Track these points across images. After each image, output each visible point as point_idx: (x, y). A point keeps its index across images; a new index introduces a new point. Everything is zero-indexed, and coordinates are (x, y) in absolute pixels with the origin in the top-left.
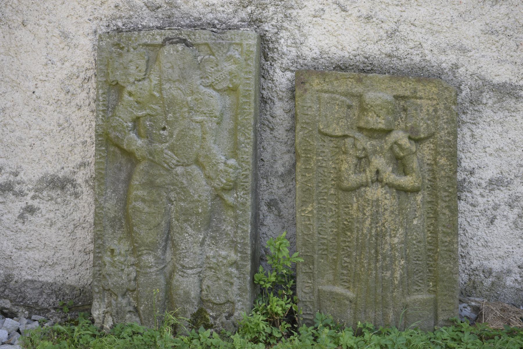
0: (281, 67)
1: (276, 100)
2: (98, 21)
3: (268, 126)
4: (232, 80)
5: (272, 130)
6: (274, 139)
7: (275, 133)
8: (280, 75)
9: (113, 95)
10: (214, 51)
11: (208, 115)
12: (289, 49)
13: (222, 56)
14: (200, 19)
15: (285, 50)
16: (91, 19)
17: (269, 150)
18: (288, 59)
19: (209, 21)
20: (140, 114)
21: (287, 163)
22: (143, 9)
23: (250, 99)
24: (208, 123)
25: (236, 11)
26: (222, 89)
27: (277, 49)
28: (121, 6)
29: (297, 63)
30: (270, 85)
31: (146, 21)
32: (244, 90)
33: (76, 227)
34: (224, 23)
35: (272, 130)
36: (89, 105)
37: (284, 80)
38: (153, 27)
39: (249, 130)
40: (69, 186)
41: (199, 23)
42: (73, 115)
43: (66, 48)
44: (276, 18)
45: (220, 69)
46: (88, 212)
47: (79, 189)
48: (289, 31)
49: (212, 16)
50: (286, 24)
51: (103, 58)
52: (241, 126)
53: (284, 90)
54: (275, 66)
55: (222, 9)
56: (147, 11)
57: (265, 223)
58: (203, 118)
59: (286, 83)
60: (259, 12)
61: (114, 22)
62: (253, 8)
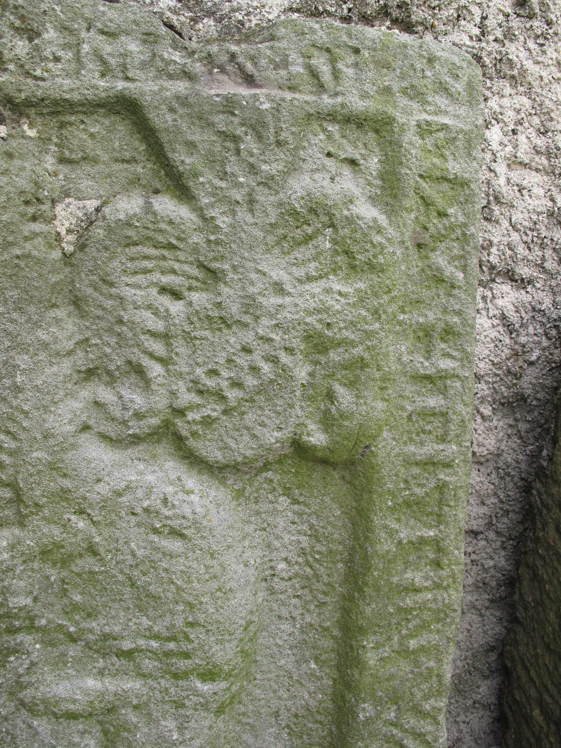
4: (330, 396)
11: (148, 664)
12: (516, 175)
13: (251, 202)
23: (440, 519)
24: (150, 719)
26: (248, 462)
29: (542, 246)
32: (408, 462)
34: (210, 14)
45: (234, 309)
48: (528, 94)
50: (523, 54)
52: (377, 702)
59: (493, 334)
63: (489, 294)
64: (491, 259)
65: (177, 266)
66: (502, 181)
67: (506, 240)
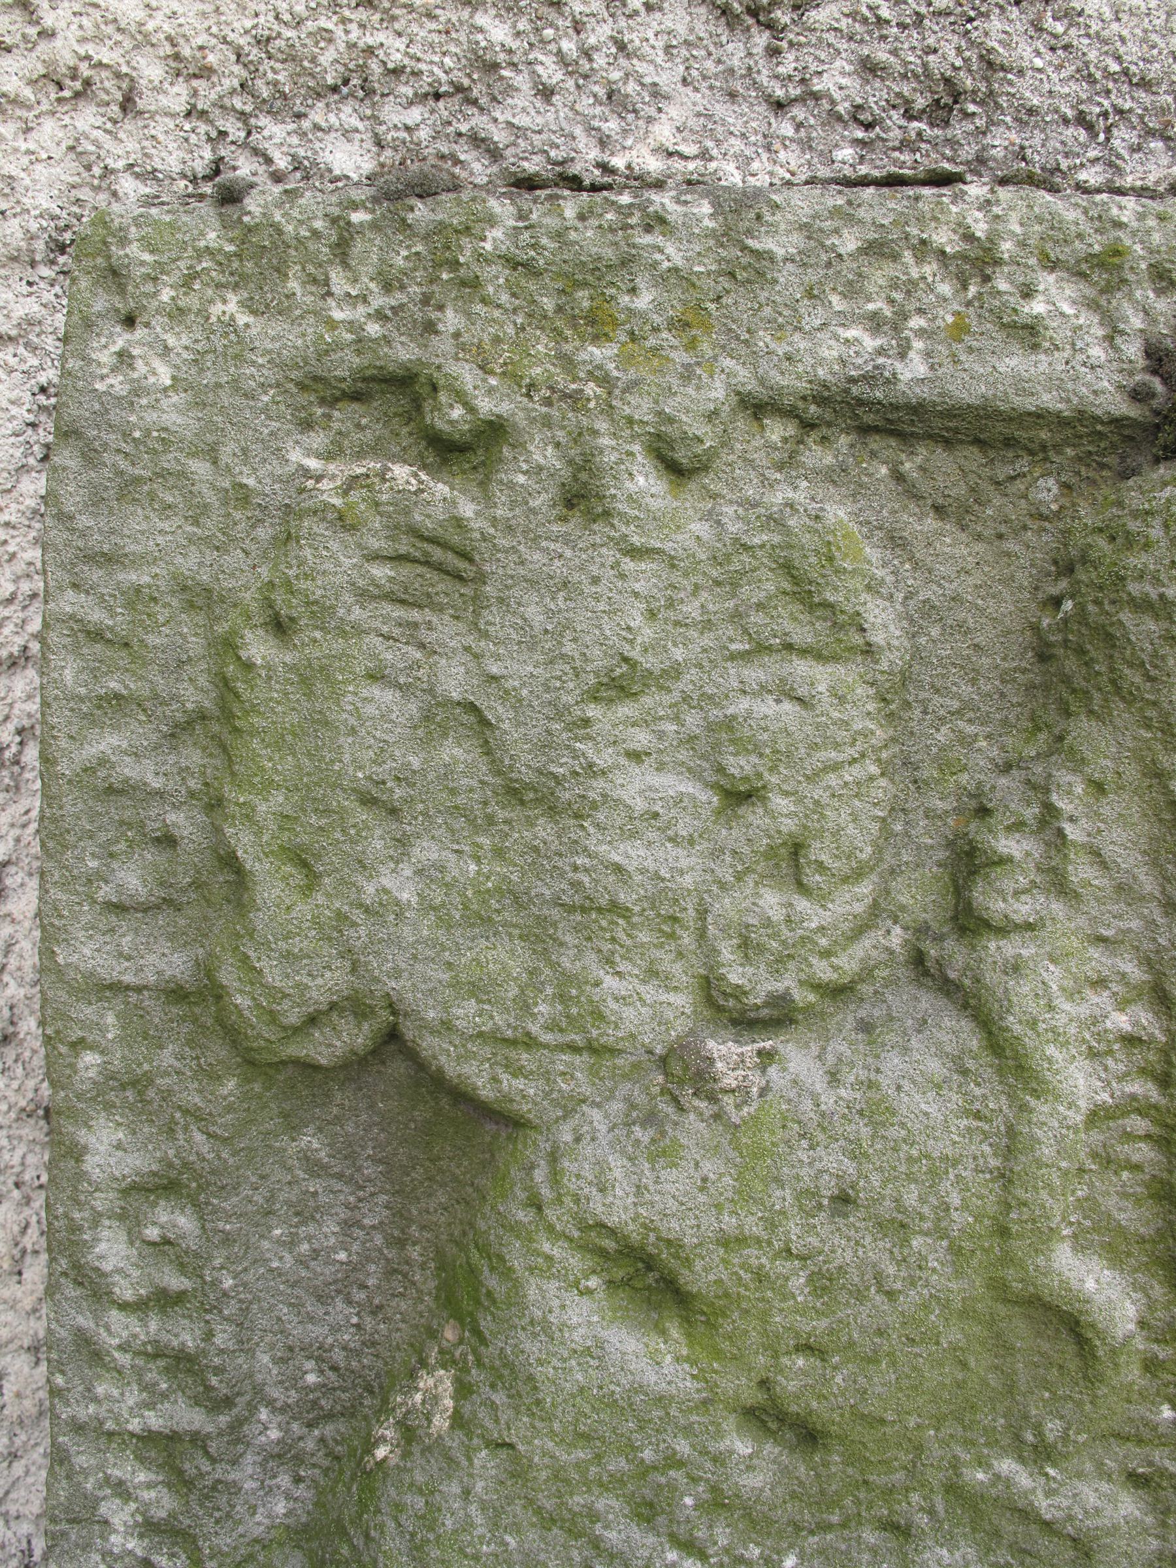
2: (87, 118)
9: (305, 1212)
31: (663, 132)
51: (136, 597)
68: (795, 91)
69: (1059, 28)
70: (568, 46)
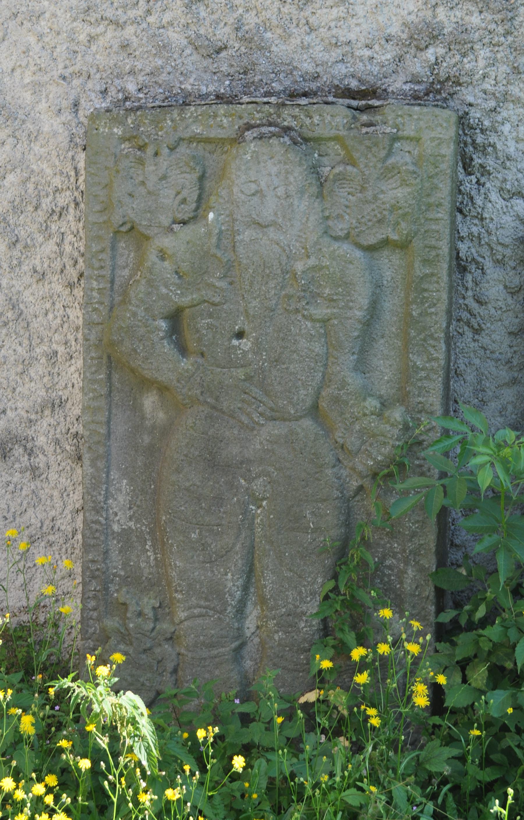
0: (501, 189)
1: (488, 264)
3: (468, 324)
5: (477, 331)
6: (482, 352)
7: (485, 340)
8: (498, 206)
10: (356, 155)
14: (316, 77)
15: (512, 150)
16: (67, 75)
17: (468, 378)
18: (519, 171)
19: (336, 82)
20: (185, 301)
21: (510, 408)
22: (185, 54)
25: (400, 59)
27: (494, 146)
28: (135, 45)
30: (475, 230)
31: (191, 80)
33: (32, 541)
35: (477, 331)
36: (62, 271)
37: (508, 220)
38: (208, 95)
39: (436, 339)
40: (18, 451)
41: (314, 86)
42: (27, 293)
43: (11, 140)
44: (493, 75)
46: (59, 510)
47: (40, 460)
49: (344, 71)
50: (517, 90)
53: (507, 241)
54: (488, 185)
55: (367, 53)
56: (195, 57)
57: (457, 541)
58: (329, 311)
60: (454, 61)
61: (117, 82)
62: (441, 51)
63: (509, 205)
64: (508, 187)
65: (353, 186)
66: (512, 150)
67: (515, 178)
68: (217, 70)
69: (268, 55)
70: (173, 64)
